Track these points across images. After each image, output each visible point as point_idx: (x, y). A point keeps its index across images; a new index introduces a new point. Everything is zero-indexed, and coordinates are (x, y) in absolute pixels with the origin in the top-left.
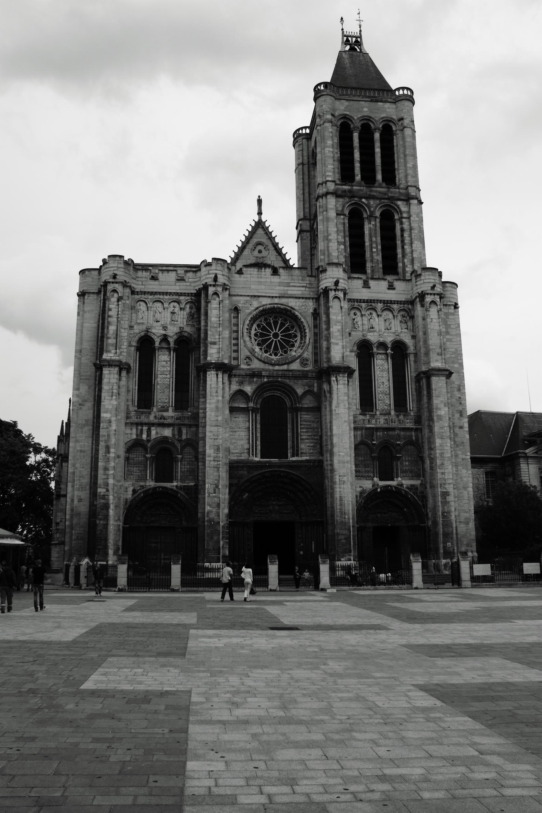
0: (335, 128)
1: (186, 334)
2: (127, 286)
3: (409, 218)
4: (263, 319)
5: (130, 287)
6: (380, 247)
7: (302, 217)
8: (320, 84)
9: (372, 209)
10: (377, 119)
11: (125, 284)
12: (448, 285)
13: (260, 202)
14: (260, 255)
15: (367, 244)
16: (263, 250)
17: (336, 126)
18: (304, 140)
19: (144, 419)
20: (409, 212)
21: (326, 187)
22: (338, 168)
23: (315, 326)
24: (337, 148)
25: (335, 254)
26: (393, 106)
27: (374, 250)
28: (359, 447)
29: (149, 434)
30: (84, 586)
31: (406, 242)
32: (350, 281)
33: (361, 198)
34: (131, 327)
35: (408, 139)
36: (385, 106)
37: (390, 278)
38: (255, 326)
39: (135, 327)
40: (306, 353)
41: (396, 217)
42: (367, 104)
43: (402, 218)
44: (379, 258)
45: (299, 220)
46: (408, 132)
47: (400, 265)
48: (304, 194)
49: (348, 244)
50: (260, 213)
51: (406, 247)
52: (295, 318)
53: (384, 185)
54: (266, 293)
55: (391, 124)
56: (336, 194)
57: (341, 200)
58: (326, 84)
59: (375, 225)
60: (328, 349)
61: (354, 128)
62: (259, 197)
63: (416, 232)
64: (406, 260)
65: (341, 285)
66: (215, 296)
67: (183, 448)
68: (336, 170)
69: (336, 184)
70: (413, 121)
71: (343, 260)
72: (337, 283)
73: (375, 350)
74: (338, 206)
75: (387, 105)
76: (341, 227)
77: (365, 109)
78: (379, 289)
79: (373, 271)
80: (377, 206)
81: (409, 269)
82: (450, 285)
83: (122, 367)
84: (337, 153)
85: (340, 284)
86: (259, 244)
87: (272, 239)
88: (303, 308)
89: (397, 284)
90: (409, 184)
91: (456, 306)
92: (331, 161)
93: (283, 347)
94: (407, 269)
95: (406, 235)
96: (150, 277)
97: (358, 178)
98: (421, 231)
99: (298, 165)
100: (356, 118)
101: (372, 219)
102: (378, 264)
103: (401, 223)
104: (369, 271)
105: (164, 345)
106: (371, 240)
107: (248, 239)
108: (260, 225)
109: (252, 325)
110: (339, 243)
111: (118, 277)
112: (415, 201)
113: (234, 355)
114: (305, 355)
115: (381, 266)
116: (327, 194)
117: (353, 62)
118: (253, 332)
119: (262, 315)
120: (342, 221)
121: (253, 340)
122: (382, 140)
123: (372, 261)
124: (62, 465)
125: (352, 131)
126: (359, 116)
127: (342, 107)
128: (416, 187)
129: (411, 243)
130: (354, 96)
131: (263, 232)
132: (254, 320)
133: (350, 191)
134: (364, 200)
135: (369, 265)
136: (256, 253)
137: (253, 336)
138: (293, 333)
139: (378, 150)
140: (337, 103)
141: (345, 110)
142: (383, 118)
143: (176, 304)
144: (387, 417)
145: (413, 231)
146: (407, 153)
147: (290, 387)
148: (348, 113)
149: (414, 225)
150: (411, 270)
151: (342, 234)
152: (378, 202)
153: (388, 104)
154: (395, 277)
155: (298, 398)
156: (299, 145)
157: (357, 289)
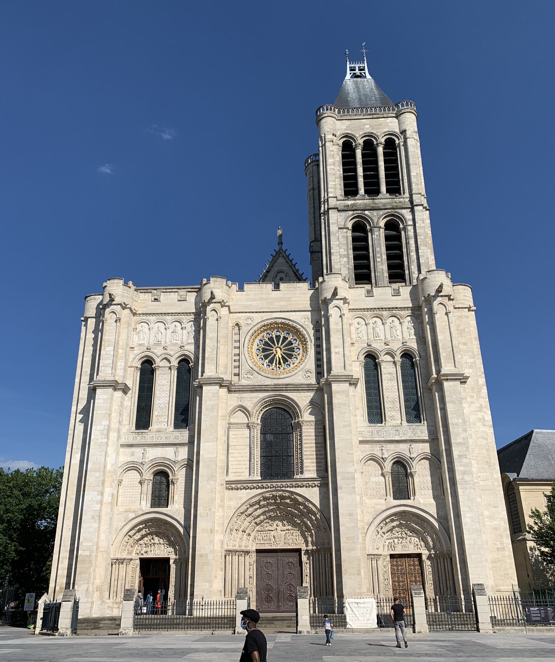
0: (337, 146)
1: (187, 353)
2: (127, 308)
4: (265, 334)
5: (130, 309)
7: (314, 239)
9: (375, 221)
10: (379, 134)
18: (314, 167)
19: (139, 439)
20: (414, 220)
22: (340, 185)
24: (339, 166)
27: (378, 260)
28: (369, 462)
36: (387, 121)
39: (136, 348)
40: (308, 365)
41: (401, 226)
44: (385, 267)
45: (311, 243)
49: (351, 256)
52: (297, 332)
54: (268, 308)
55: (393, 137)
57: (343, 214)
61: (356, 145)
63: (423, 237)
71: (347, 272)
81: (415, 275)
93: (285, 361)
95: (412, 242)
96: (153, 300)
97: (362, 191)
100: (357, 135)
101: (376, 229)
105: (165, 363)
110: (341, 256)
113: (236, 371)
114: (307, 367)
119: (265, 330)
121: (255, 355)
122: (385, 154)
125: (355, 148)
126: (361, 133)
130: (356, 115)
131: (284, 261)
132: (255, 334)
133: (353, 205)
134: (366, 212)
138: (296, 346)
141: (346, 129)
145: (418, 237)
147: (293, 400)
148: (349, 132)
152: (381, 212)
153: (389, 119)
154: (404, 284)
155: (300, 412)
156: (309, 173)
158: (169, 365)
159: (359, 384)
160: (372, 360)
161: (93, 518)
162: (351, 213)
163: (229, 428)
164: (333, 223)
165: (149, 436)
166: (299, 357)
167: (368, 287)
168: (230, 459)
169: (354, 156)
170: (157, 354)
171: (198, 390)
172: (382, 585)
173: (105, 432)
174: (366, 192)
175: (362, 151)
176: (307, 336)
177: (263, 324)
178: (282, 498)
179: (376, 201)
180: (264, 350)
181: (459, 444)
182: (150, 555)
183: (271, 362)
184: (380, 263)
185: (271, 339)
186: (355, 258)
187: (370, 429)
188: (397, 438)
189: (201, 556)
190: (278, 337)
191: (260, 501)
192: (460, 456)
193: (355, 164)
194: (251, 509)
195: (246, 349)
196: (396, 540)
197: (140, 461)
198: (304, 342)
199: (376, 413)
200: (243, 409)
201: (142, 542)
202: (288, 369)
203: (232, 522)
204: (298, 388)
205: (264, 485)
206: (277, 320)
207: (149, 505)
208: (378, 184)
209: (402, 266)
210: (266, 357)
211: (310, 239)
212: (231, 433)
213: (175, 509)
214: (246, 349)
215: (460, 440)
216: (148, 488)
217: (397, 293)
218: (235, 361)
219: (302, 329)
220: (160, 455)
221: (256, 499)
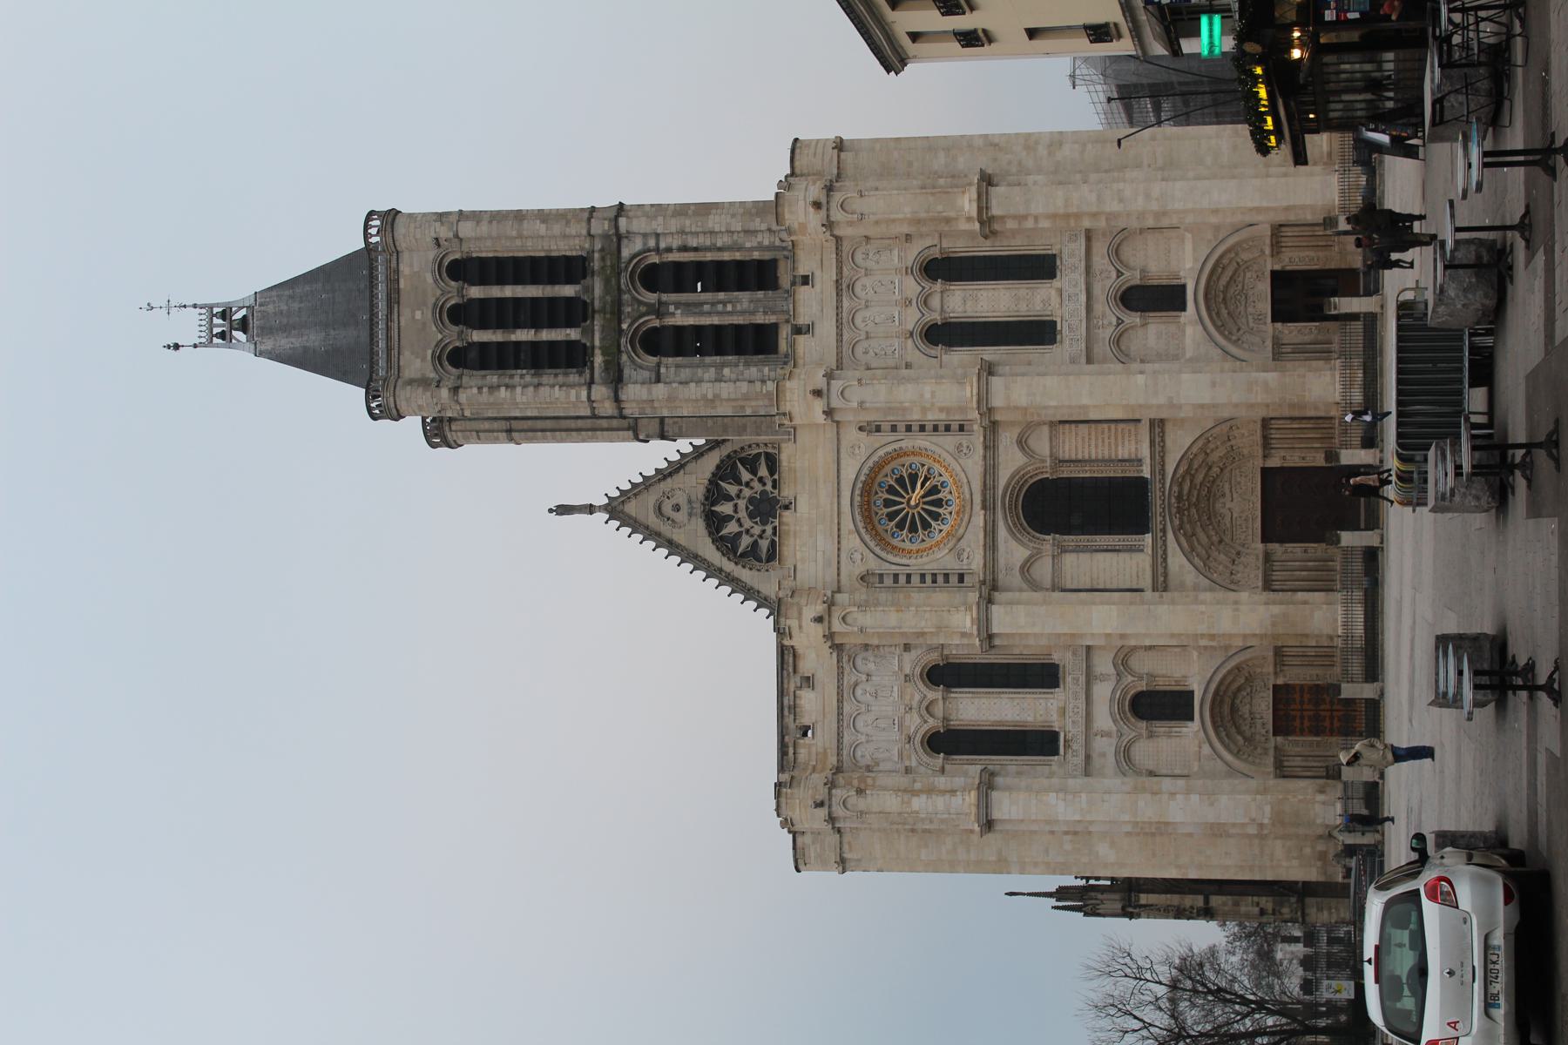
0: (465, 379)
1: (918, 670)
3: (657, 235)
4: (880, 528)
6: (721, 295)
7: (631, 433)
8: (369, 410)
9: (643, 309)
11: (831, 785)
12: (797, 164)
13: (563, 510)
14: (685, 509)
15: (716, 320)
16: (674, 501)
17: (460, 377)
19: (1079, 746)
20: (645, 235)
21: (602, 401)
23: (894, 429)
24: (512, 376)
25: (744, 387)
26: (405, 257)
27: (729, 308)
29: (1107, 734)
30: (1378, 837)
31: (708, 243)
32: (800, 362)
33: (621, 331)
34: (908, 770)
35: (484, 228)
37: (785, 280)
38: (895, 542)
39: (907, 763)
41: (655, 259)
42: (406, 313)
43: (657, 250)
46: (466, 229)
47: (756, 255)
48: (579, 430)
50: (590, 509)
51: (719, 244)
53: (588, 281)
56: (616, 380)
57: (626, 372)
58: (371, 395)
59: (678, 305)
60: (941, 410)
62: (551, 511)
63: (688, 222)
64: (748, 245)
65: (820, 382)
66: (849, 619)
67: (1131, 672)
68: (561, 379)
69: (591, 383)
70: (441, 217)
71: (754, 370)
72: (817, 393)
73: (936, 317)
74: (640, 378)
75: (405, 269)
76: (685, 373)
77: (418, 315)
78: (813, 304)
79: (774, 313)
80: (634, 298)
82: (797, 157)
83: (987, 785)
84: (522, 376)
85: (818, 387)
86: (659, 510)
87: (647, 483)
88: (859, 454)
89: (802, 270)
90: (584, 232)
91: (840, 145)
92: (545, 391)
94: (766, 243)
95: (693, 242)
97: (573, 334)
98: (682, 210)
99: (511, 440)
102: (759, 300)
103: (669, 250)
104: (772, 319)
106: (709, 313)
107: (650, 534)
108: (616, 509)
109: (894, 548)
111: (819, 798)
112: (622, 222)
113: (954, 579)
114: (951, 449)
115: (760, 294)
116: (617, 400)
117: (286, 329)
118: (907, 545)
120: (672, 370)
122: (483, 281)
123: (753, 313)
124: (1145, 906)
127: (416, 363)
128: (589, 220)
129: (711, 232)
133: (603, 354)
134: (625, 326)
135: (760, 319)
136: (680, 517)
137: (914, 547)
139: (509, 291)
140: (408, 373)
141: (424, 359)
142: (435, 281)
143: (859, 692)
144: (1065, 295)
146: (514, 233)
147: (1012, 477)
149: (674, 225)
150: (767, 235)
151: (700, 371)
152: (626, 297)
157: (814, 349)
158: (941, 702)
159: (986, 357)
160: (943, 334)
161: (1212, 804)
162: (624, 357)
163: (1064, 590)
164: (650, 392)
165: (1070, 728)
166: (928, 462)
167: (784, 332)
168: (1114, 586)
169: (483, 346)
170: (918, 725)
171: (997, 642)
172: (1320, 337)
173: (1070, 797)
174: (570, 324)
175: (474, 328)
176: (889, 449)
177: (863, 531)
178: (1179, 498)
179: (597, 304)
180: (913, 529)
181: (1099, 198)
182: (1269, 717)
183: (936, 516)
184: (740, 308)
185: (891, 516)
186: (720, 352)
187: (1067, 342)
188: (1083, 298)
189: (1274, 624)
190: (887, 503)
191: (1185, 535)
192: (1121, 200)
193: (500, 345)
194: (1199, 549)
195: (912, 561)
196: (1250, 310)
197: (1114, 741)
198: (900, 454)
199: (1039, 332)
200: (1026, 568)
201: (1248, 734)
202: (951, 486)
203: (1219, 580)
204: (990, 470)
205: (1160, 527)
206: (856, 504)
207: (1189, 724)
208: (552, 301)
209: (739, 264)
210: (926, 526)
211: (624, 440)
212: (1069, 586)
213: (1196, 677)
214: (912, 561)
215: (1093, 198)
216: (1161, 727)
217: (805, 280)
218: (934, 581)
219: (875, 458)
220: (1106, 709)
221: (1183, 540)
